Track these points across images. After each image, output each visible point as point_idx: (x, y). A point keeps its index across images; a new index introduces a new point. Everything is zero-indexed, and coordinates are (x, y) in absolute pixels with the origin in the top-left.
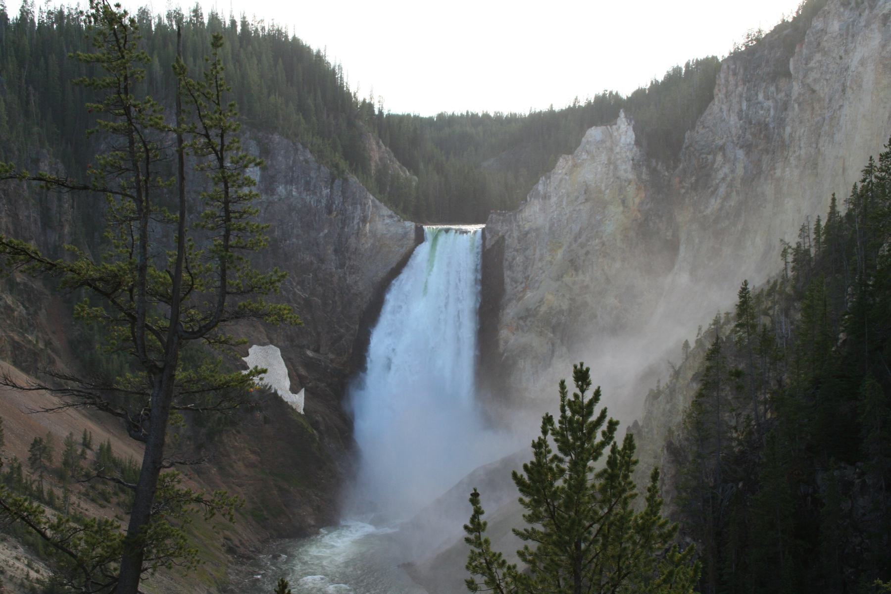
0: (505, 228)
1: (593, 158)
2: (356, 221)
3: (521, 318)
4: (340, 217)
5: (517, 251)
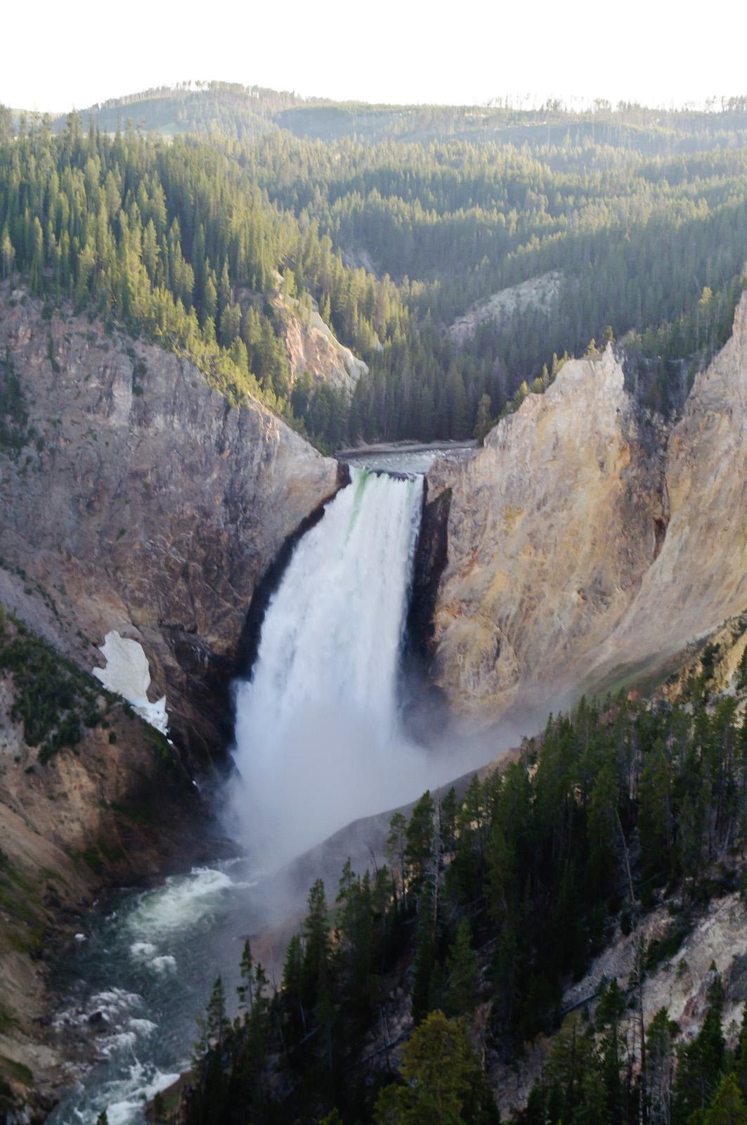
0: (453, 479)
1: (568, 402)
2: (256, 461)
3: (464, 601)
4: (234, 456)
5: (465, 513)
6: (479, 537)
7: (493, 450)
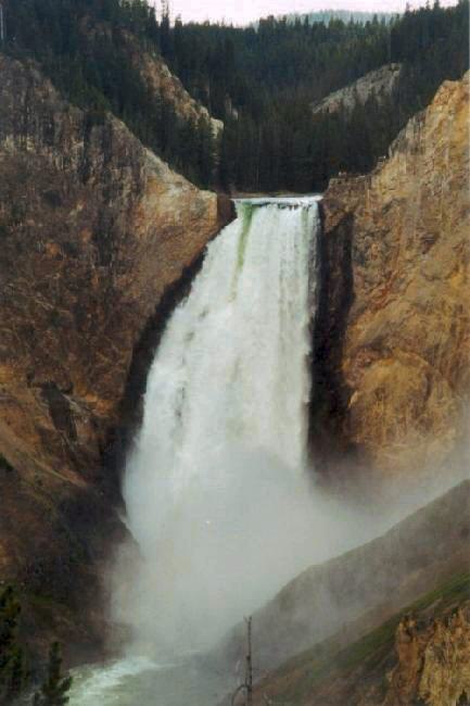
0: (354, 199)
2: (126, 191)
5: (372, 235)
6: (391, 262)
7: (402, 156)
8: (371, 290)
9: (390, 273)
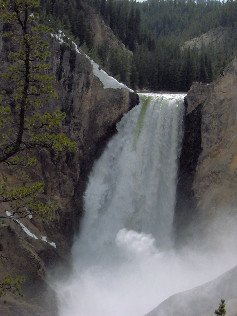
0: (204, 97)
2: (81, 86)
3: (215, 173)
5: (213, 117)
6: (223, 132)
8: (211, 147)
9: (222, 137)
